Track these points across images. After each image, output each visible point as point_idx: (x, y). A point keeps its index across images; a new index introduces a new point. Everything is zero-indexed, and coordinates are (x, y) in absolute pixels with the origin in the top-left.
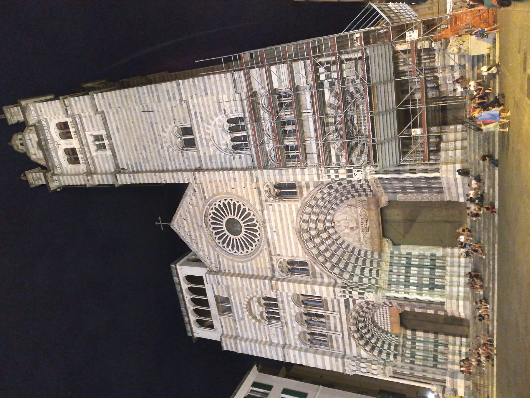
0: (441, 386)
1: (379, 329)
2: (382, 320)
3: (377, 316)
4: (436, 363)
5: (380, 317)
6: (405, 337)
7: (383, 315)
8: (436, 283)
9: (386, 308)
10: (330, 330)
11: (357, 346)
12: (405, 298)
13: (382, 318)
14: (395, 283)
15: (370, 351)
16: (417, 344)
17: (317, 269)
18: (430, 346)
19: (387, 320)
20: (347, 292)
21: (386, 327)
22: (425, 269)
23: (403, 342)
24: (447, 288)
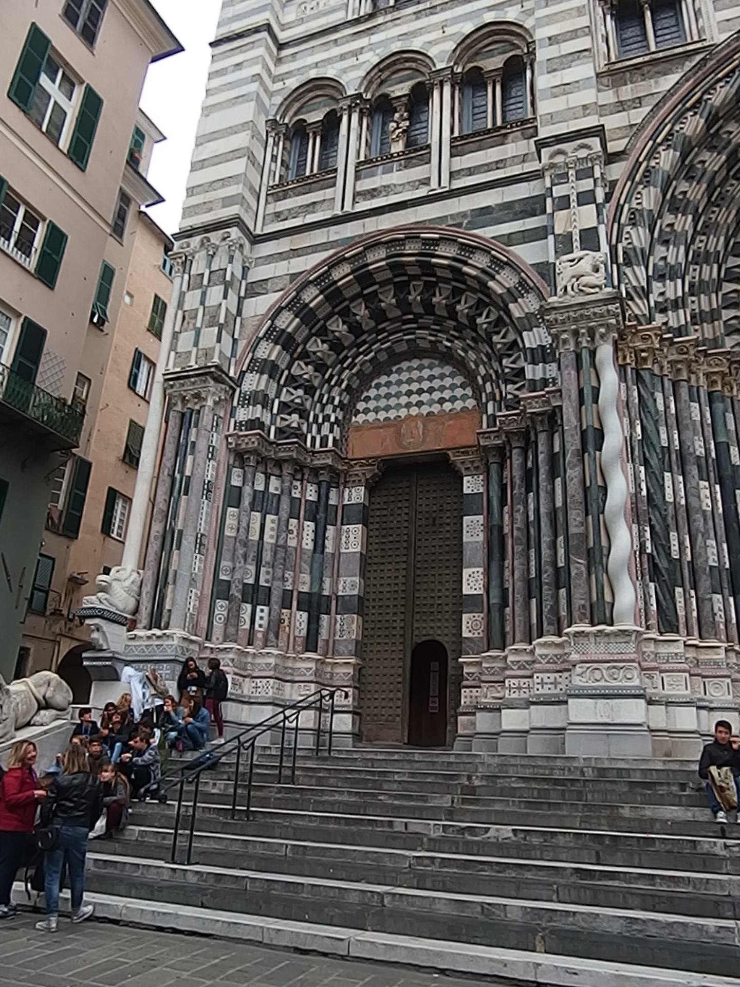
0: (136, 611)
1: (365, 380)
2: (404, 388)
3: (420, 368)
4: (235, 592)
5: (420, 380)
6: (337, 478)
7: (431, 390)
8: (679, 590)
9: (464, 398)
10: (357, 178)
11: (293, 276)
12: (600, 434)
13: (415, 387)
14: (650, 403)
15: (272, 328)
16: (309, 526)
17: (668, 82)
18: (306, 577)
19: (408, 405)
20: (586, 184)
21: (372, 404)
22: (725, 546)
23: (315, 471)
24: (676, 646)
